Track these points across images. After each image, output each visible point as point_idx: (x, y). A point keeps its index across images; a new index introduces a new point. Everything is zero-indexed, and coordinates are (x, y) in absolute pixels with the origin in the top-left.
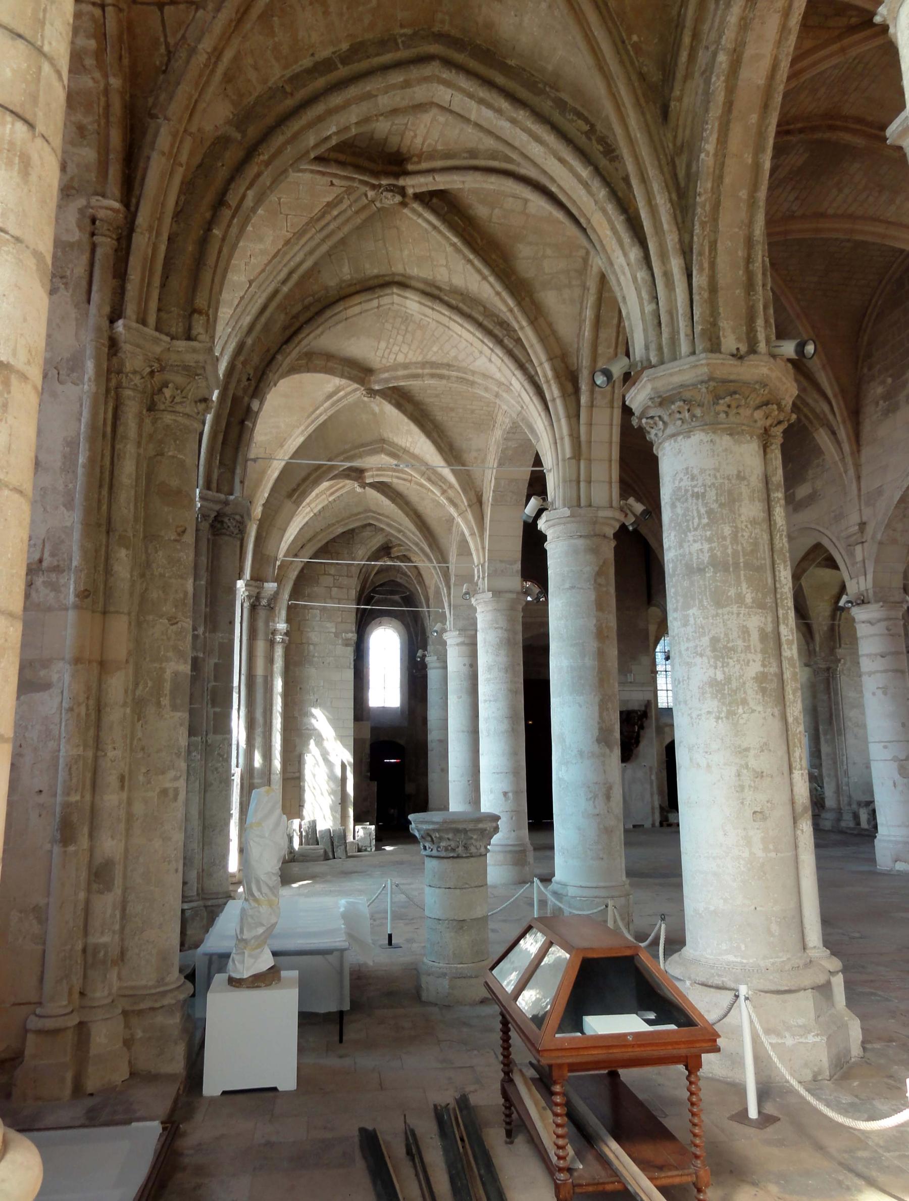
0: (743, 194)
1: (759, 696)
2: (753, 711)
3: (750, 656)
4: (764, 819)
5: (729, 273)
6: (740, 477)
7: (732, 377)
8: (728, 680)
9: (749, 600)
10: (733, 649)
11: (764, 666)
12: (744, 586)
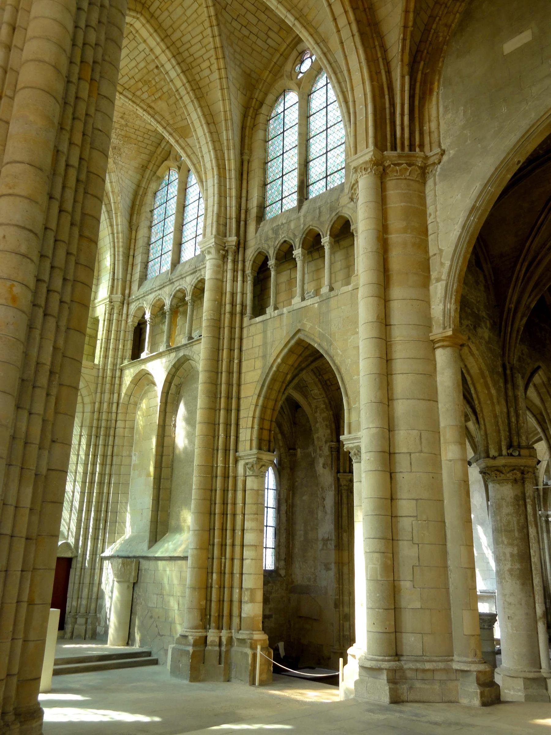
0: (489, 402)
1: (510, 577)
2: (507, 582)
3: (506, 562)
4: (512, 619)
5: (490, 429)
6: (503, 499)
7: (494, 465)
8: (500, 570)
9: (506, 543)
10: (501, 560)
11: (512, 565)
12: (504, 538)
